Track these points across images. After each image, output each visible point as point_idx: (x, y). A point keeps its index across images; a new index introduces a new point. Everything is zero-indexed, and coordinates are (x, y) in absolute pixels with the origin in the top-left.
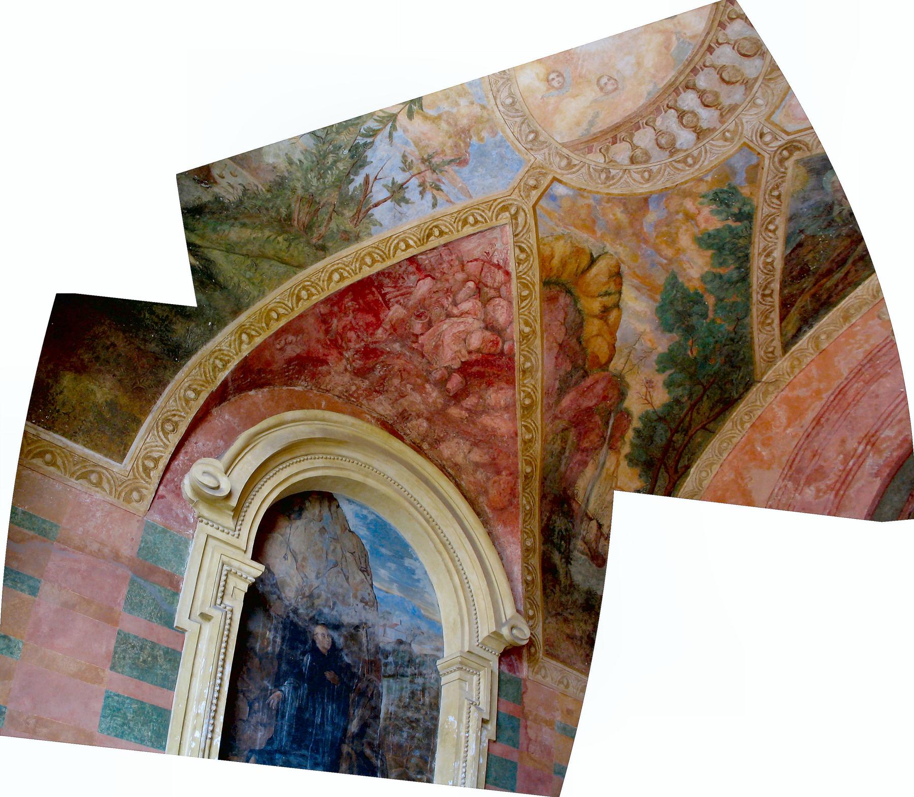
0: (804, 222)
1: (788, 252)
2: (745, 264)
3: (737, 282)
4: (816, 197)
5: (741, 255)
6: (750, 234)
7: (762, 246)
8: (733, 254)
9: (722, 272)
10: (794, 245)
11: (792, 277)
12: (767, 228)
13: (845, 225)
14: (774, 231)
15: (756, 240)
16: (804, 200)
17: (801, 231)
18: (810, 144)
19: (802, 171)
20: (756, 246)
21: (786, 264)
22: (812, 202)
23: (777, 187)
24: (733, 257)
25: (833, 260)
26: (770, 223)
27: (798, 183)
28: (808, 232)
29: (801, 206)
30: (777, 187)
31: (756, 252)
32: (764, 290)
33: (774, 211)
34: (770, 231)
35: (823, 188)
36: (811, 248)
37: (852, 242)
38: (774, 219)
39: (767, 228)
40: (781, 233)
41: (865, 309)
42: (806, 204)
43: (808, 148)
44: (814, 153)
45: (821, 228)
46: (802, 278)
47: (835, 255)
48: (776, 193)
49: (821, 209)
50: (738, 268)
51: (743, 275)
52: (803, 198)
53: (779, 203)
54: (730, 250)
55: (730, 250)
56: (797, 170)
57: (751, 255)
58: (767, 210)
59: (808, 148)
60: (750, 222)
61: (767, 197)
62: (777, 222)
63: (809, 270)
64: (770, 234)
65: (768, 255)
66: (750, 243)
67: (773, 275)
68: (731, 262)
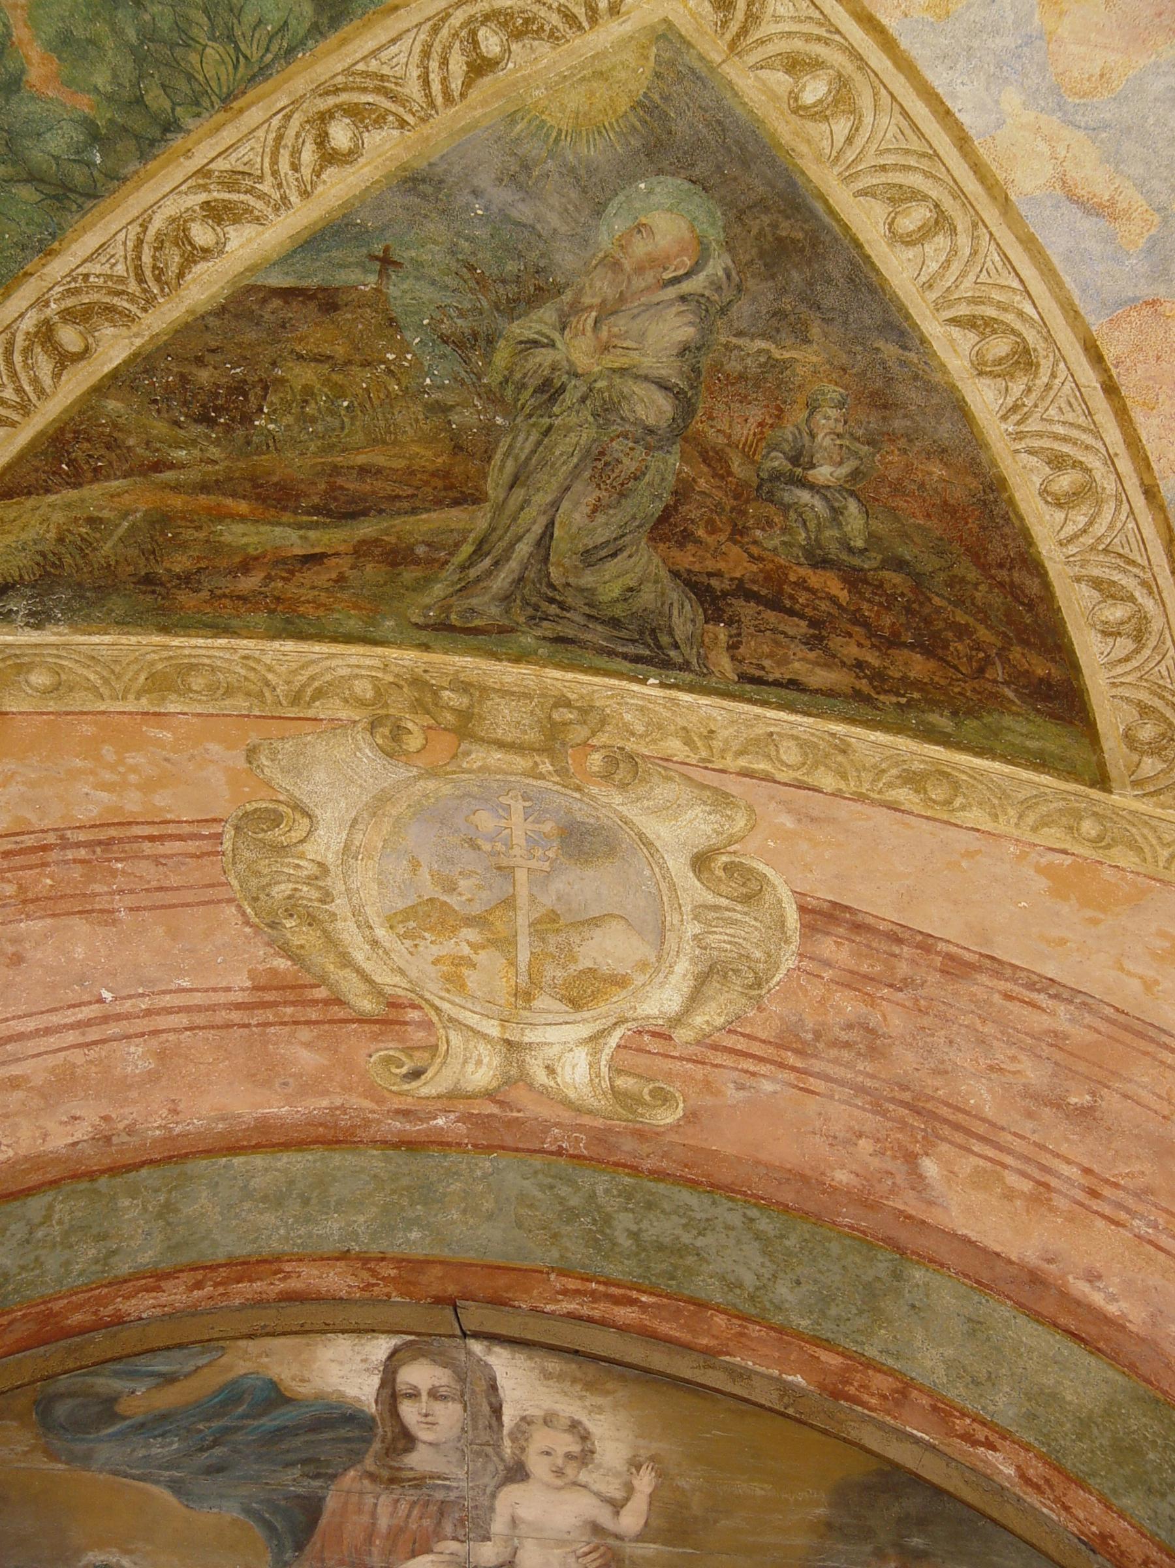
0: (429, 245)
1: (277, 280)
2: (126, 145)
3: (33, 178)
4: (550, 213)
5: (156, 99)
6: (261, 73)
7: (250, 155)
8: (140, 60)
9: (34, 74)
10: (312, 282)
11: (183, 378)
12: (325, 117)
13: (493, 398)
14: (330, 157)
15: (255, 115)
16: (521, 175)
17: (386, 262)
18: (767, 28)
19: (635, 77)
20: (228, 136)
21: (221, 311)
22: (524, 212)
23: (520, 28)
24: (128, 70)
25: (336, 470)
26: (354, 112)
27: (575, 100)
28: (398, 289)
29: (484, 180)
30: (520, 28)
31: (202, 155)
32: (68, 315)
33: (413, 89)
34: (322, 140)
35: (599, 210)
36: (340, 350)
37: (444, 474)
38: (380, 121)
39: (325, 117)
40: (338, 188)
41: (240, 704)
42: (502, 196)
43: (744, 31)
44: (732, 71)
45: (435, 323)
46: (204, 419)
47: (361, 459)
48: (491, 42)
49: (511, 267)
50: (95, 136)
51: (79, 175)
52: (526, 167)
53: (456, 85)
54: (148, 34)
55: (148, 34)
56: (629, 57)
57: (178, 142)
58: (401, 62)
59: (744, 31)
60: (317, 31)
61: (458, 18)
62: (374, 138)
63: (246, 419)
64: (308, 155)
65: (216, 213)
66: (228, 99)
67: (149, 302)
68: (101, 79)
